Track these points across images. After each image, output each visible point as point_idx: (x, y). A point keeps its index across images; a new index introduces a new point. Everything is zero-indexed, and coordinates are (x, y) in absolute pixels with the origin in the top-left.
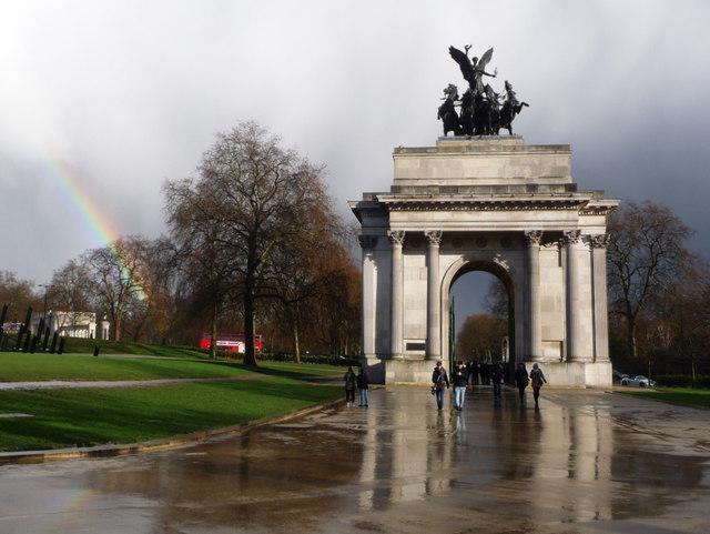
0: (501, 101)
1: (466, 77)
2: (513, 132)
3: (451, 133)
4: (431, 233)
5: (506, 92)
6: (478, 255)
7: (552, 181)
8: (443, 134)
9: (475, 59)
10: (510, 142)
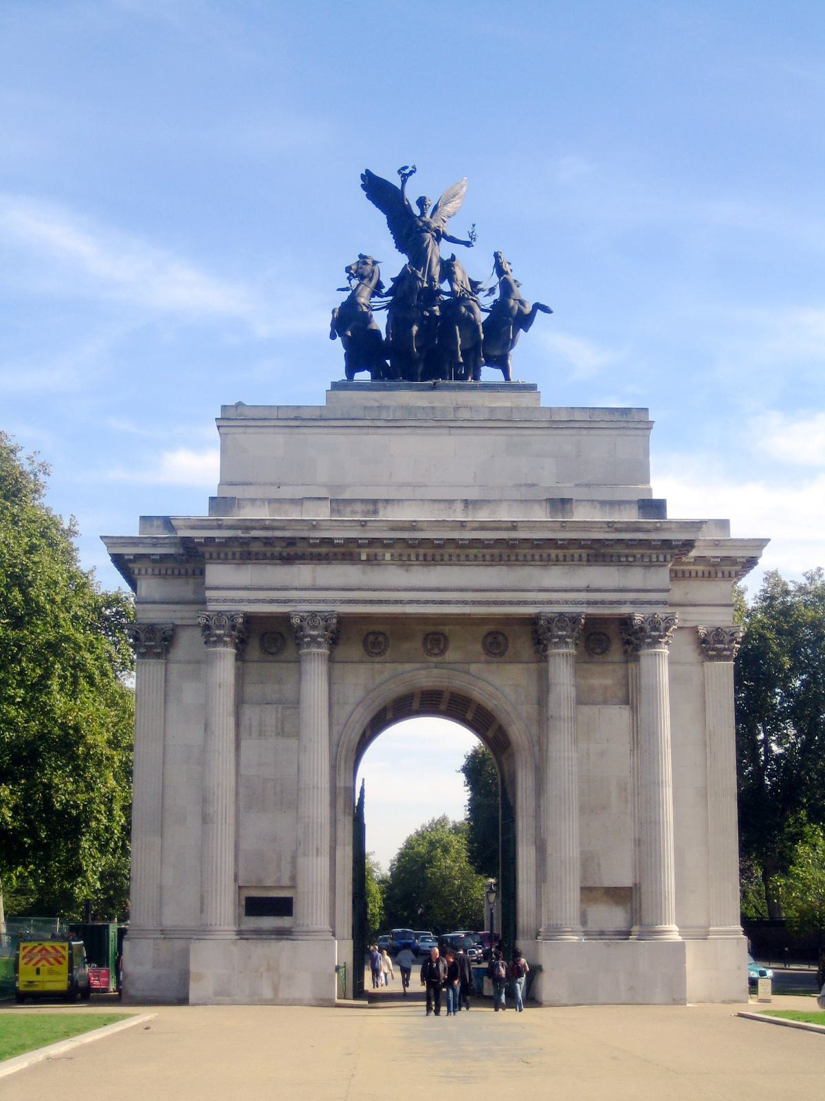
0: (487, 301)
1: (401, 246)
2: (514, 377)
3: (364, 376)
4: (313, 614)
5: (494, 281)
6: (425, 676)
7: (605, 494)
8: (341, 376)
9: (421, 202)
10: (505, 400)
